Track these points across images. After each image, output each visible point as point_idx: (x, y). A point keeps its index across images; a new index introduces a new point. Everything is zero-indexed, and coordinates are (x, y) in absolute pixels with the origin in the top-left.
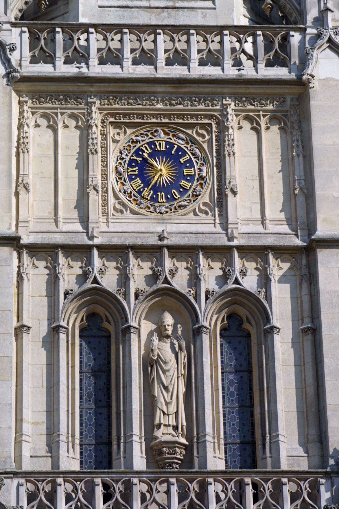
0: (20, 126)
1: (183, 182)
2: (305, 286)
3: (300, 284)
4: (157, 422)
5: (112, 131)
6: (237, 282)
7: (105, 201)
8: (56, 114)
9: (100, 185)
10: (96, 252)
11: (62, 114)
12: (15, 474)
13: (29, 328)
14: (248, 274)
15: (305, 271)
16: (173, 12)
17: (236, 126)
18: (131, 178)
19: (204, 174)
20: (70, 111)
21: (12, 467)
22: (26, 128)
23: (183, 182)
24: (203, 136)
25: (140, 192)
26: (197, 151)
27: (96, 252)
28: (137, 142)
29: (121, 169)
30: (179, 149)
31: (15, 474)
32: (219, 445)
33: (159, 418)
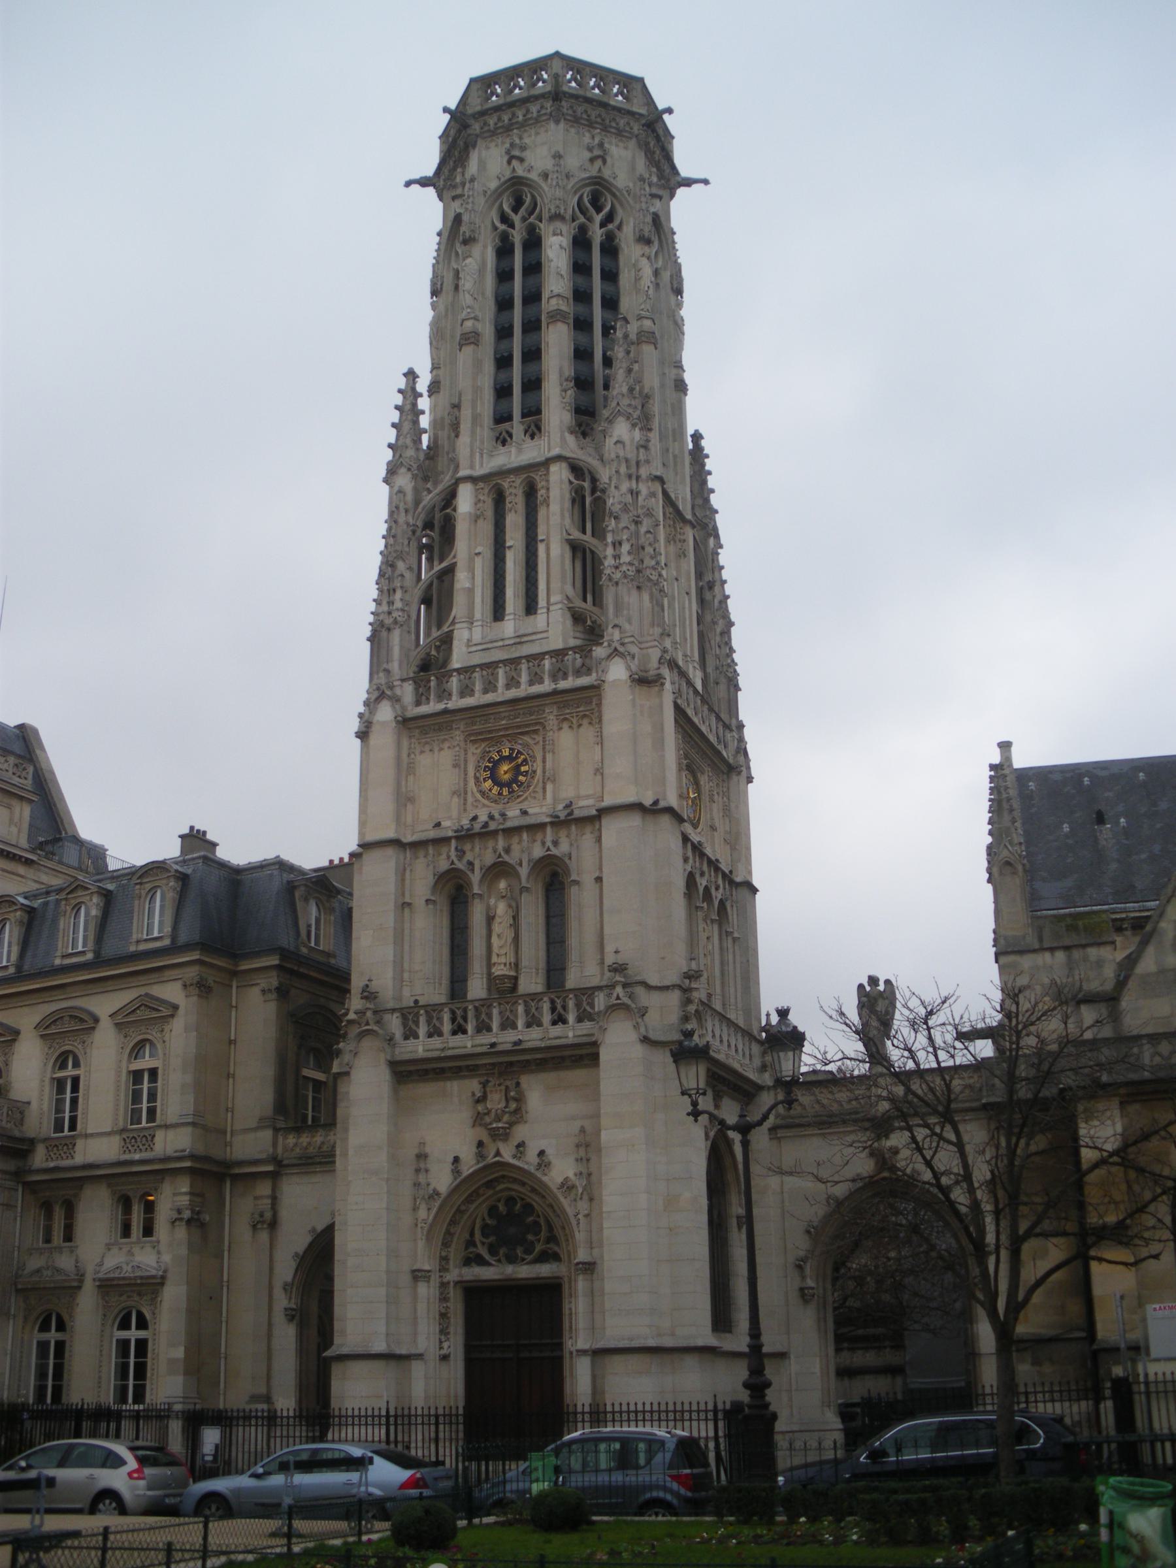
0: (409, 755)
1: (521, 778)
2: (597, 845)
4: (493, 962)
6: (548, 849)
7: (465, 800)
9: (462, 790)
13: (409, 904)
14: (560, 840)
15: (597, 834)
16: (519, 646)
17: (555, 728)
18: (485, 780)
19: (534, 769)
20: (442, 737)
21: (391, 1005)
22: (412, 756)
23: (521, 778)
24: (534, 739)
25: (490, 790)
26: (530, 752)
28: (490, 751)
29: (478, 774)
30: (519, 752)
31: (393, 1010)
32: (537, 974)
33: (494, 959)
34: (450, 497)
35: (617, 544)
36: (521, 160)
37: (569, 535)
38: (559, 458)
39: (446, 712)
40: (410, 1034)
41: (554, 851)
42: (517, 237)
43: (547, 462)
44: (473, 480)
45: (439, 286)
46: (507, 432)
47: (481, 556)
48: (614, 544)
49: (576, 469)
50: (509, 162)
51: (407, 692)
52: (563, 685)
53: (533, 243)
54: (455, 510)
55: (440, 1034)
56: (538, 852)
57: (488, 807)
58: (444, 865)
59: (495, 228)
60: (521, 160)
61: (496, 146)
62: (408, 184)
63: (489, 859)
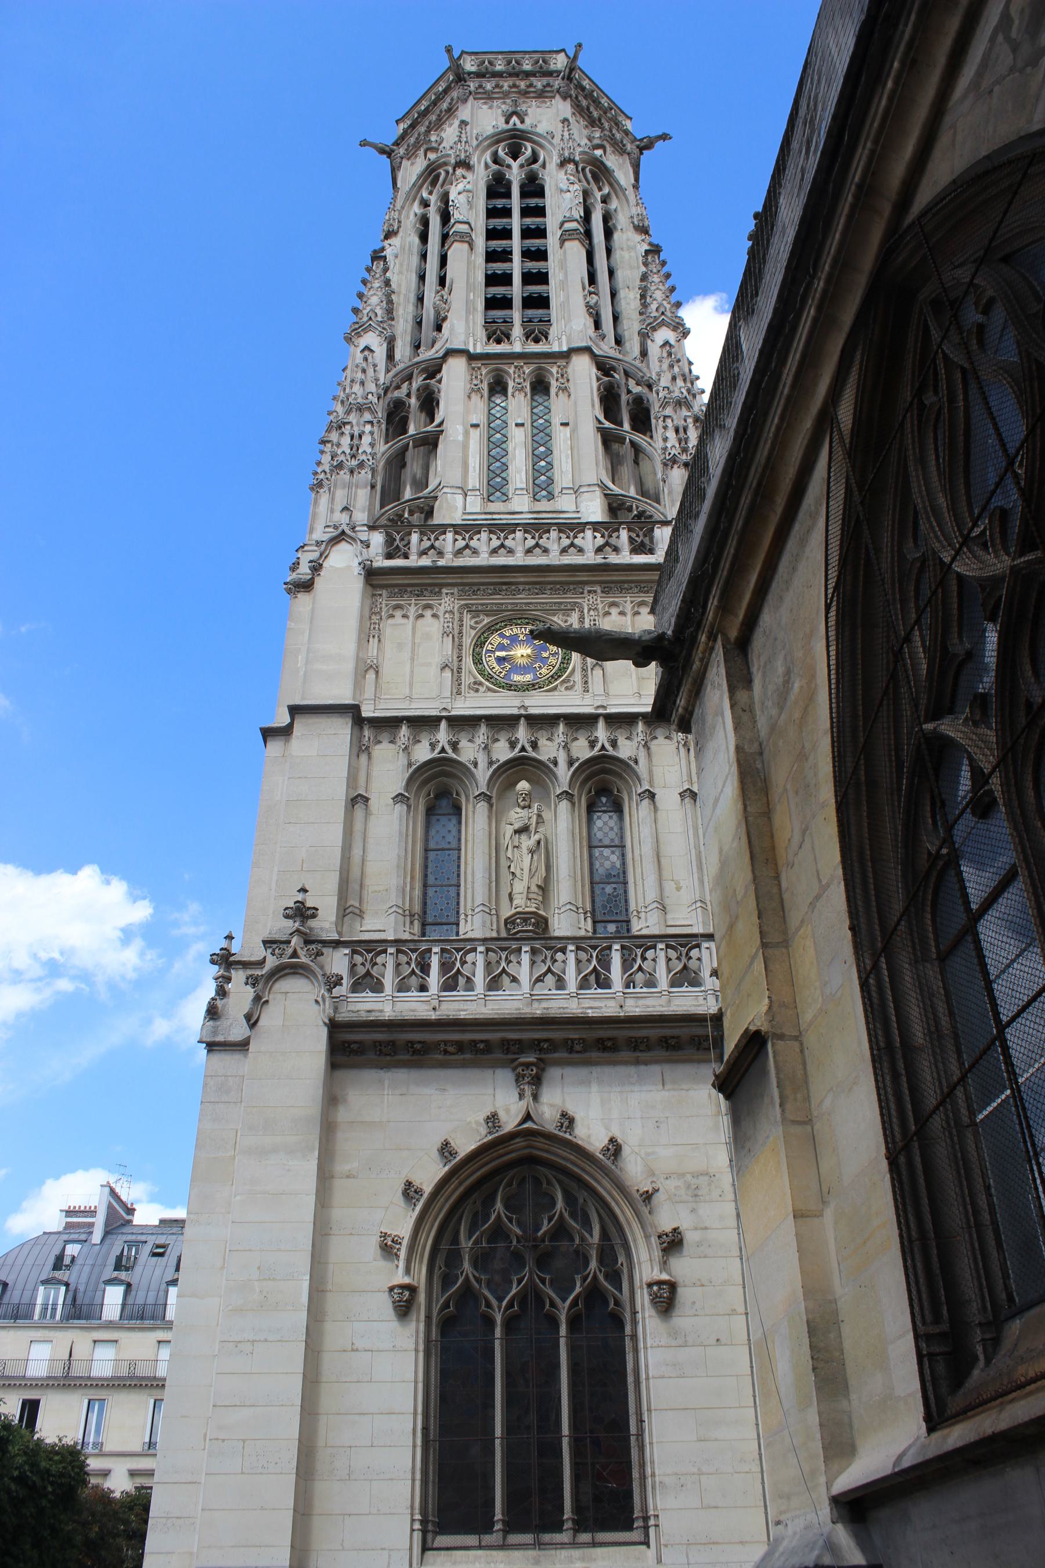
3: (678, 748)
5: (468, 620)
8: (410, 605)
10: (443, 724)
11: (416, 605)
12: (337, 944)
13: (367, 800)
27: (443, 724)
31: (337, 944)
34: (433, 370)
35: (681, 430)
36: (522, 122)
37: (600, 422)
38: (588, 350)
39: (435, 570)
40: (366, 982)
41: (611, 751)
42: (515, 174)
43: (566, 355)
44: (472, 357)
45: (396, 228)
46: (502, 333)
47: (479, 429)
48: (677, 431)
49: (604, 367)
50: (507, 122)
51: (377, 539)
52: (614, 559)
53: (533, 188)
54: (440, 381)
55: (423, 988)
56: (582, 750)
57: (495, 691)
58: (423, 753)
59: (487, 166)
60: (522, 122)
61: (491, 108)
62: (364, 143)
63: (503, 752)
